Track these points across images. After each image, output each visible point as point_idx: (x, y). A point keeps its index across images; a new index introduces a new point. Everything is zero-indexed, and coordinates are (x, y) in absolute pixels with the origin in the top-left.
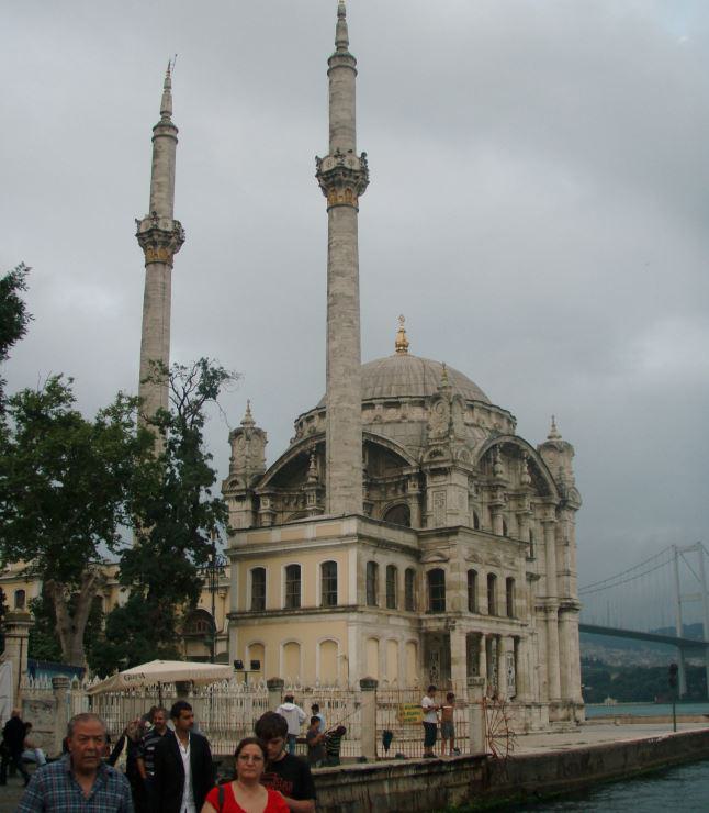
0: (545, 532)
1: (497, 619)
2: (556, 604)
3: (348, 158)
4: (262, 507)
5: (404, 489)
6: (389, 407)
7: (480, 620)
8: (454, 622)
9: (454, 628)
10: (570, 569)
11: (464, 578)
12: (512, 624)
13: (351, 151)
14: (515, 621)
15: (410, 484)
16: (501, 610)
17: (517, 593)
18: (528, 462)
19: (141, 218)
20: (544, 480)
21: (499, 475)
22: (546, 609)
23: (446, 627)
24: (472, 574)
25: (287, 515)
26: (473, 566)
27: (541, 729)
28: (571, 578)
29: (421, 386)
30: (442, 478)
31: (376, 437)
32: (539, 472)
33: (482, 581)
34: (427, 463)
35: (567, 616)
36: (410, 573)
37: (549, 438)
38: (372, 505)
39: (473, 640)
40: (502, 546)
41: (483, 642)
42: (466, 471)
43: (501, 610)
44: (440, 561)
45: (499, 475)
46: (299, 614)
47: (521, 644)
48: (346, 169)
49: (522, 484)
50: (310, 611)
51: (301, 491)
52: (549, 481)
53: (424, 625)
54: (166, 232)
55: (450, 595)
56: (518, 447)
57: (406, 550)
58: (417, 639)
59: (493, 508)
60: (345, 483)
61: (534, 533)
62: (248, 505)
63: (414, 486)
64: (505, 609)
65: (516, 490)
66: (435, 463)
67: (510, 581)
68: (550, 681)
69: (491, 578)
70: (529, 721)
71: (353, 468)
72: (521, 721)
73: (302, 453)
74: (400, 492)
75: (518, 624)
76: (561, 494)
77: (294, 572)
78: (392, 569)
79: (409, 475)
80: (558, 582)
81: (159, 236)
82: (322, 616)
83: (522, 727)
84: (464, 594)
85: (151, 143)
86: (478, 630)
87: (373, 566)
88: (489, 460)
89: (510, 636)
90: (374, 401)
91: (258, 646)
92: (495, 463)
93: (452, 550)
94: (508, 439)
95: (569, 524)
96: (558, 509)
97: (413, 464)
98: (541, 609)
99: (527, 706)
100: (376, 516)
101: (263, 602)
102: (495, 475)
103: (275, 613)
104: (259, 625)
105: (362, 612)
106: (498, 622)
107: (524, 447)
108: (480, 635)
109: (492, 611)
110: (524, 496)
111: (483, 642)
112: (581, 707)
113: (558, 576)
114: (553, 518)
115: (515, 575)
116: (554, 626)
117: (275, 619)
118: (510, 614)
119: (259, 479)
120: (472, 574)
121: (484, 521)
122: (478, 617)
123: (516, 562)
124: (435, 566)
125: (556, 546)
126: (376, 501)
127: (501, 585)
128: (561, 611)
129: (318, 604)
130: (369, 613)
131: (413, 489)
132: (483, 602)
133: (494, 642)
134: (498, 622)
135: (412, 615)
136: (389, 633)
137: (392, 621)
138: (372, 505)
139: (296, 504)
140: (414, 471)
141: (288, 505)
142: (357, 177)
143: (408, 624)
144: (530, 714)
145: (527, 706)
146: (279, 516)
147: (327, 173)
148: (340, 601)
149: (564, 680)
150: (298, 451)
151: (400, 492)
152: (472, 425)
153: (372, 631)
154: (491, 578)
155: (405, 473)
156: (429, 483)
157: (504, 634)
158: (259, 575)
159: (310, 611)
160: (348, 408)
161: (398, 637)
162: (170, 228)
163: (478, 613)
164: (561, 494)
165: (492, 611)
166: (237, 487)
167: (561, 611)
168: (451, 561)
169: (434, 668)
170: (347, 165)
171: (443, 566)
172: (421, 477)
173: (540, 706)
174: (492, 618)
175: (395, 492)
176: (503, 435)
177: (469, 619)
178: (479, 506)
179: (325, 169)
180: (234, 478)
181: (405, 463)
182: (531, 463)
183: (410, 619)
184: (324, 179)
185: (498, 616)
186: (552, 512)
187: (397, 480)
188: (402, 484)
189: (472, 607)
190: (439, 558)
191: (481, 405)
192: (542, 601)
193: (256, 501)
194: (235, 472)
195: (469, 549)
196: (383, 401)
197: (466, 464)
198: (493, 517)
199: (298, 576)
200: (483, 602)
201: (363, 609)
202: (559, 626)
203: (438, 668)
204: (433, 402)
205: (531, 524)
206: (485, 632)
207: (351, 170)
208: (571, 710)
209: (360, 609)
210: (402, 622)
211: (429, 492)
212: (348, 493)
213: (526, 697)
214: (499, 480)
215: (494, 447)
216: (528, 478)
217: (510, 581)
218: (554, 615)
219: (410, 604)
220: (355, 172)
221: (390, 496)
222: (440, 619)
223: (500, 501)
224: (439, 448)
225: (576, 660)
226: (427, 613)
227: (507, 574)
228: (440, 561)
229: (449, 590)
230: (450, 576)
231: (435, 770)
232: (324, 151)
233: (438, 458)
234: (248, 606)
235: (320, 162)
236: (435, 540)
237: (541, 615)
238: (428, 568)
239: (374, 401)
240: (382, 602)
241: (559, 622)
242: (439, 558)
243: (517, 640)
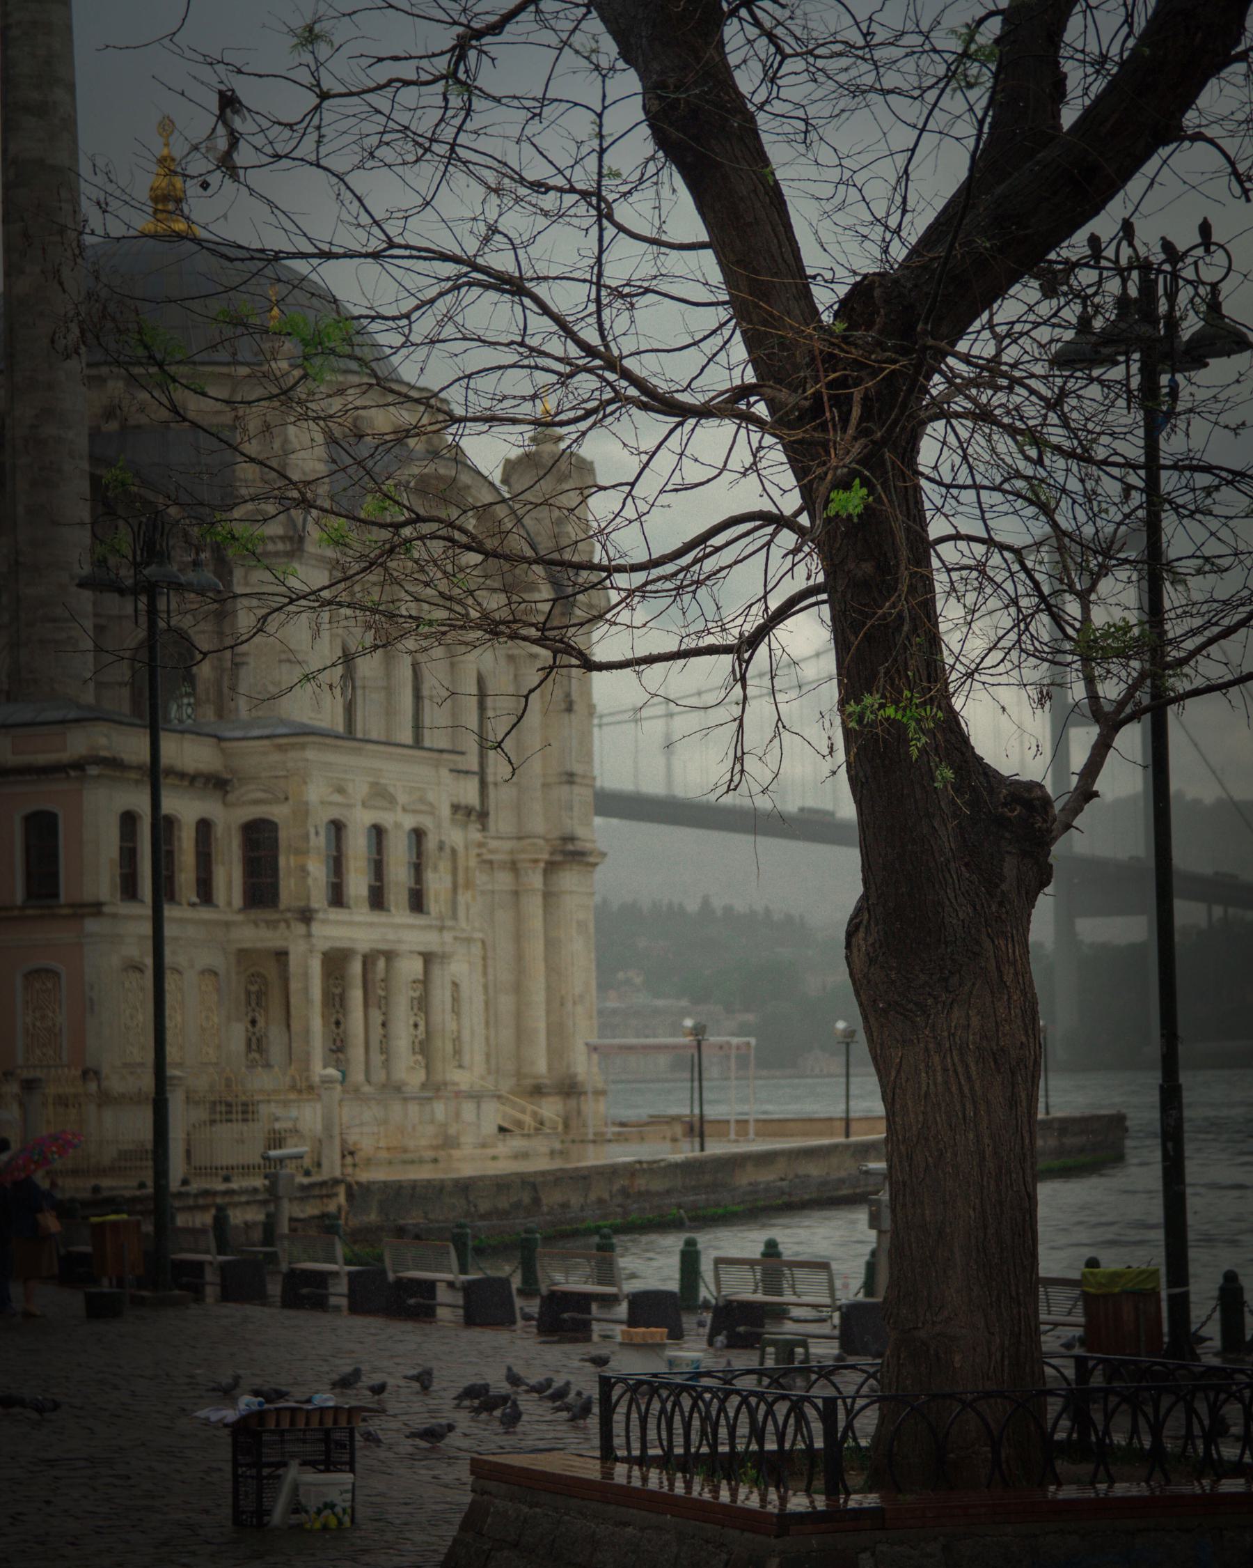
28: (577, 789)
33: (358, 846)
35: (569, 879)
36: (204, 826)
39: (335, 962)
41: (356, 967)
47: (436, 971)
64: (404, 897)
67: (418, 835)
68: (521, 1034)
70: (452, 1131)
75: (430, 927)
84: (318, 870)
109: (377, 900)
111: (356, 967)
115: (427, 822)
116: (534, 906)
118: (417, 902)
125: (545, 713)
128: (551, 868)
132: (358, 884)
133: (381, 963)
149: (558, 1033)
157: (404, 947)
165: (377, 900)
171: (278, 812)
189: (337, 897)
192: (508, 845)
200: (358, 884)
209: (106, 909)
218: (536, 880)
227: (409, 822)
237: (504, 880)
243: (428, 958)
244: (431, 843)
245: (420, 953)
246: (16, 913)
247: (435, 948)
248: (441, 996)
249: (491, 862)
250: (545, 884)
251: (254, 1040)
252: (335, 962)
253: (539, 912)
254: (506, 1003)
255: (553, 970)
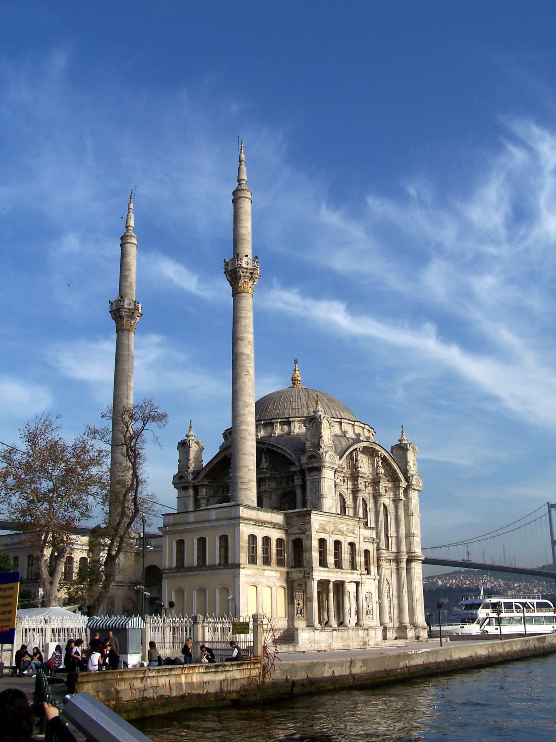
0: (396, 508)
1: (342, 570)
2: (405, 557)
3: (245, 259)
4: (199, 494)
5: (293, 481)
6: (284, 425)
7: (328, 571)
8: (309, 574)
9: (308, 578)
10: (415, 532)
11: (315, 544)
12: (353, 573)
13: (247, 256)
14: (355, 571)
15: (295, 477)
16: (346, 564)
17: (357, 552)
18: (382, 459)
19: (113, 300)
20: (395, 471)
21: (359, 469)
22: (397, 561)
23: (304, 577)
24: (322, 542)
25: (216, 499)
26: (323, 536)
27: (376, 644)
29: (305, 409)
30: (316, 473)
31: (273, 446)
32: (390, 465)
33: (330, 547)
34: (305, 464)
37: (399, 441)
38: (272, 492)
40: (344, 521)
42: (332, 468)
43: (346, 564)
44: (300, 533)
45: (359, 469)
46: (205, 570)
47: (360, 587)
48: (242, 268)
49: (377, 474)
50: (213, 567)
51: (224, 482)
52: (398, 471)
53: (290, 576)
54: (129, 309)
55: (306, 555)
56: (374, 450)
57: (275, 526)
58: (285, 585)
59: (355, 492)
60: (244, 480)
61: (388, 508)
62: (191, 492)
63: (298, 479)
65: (373, 479)
66: (313, 462)
67: (352, 545)
69: (337, 544)
70: (366, 640)
71: (249, 470)
72: (360, 639)
73: (226, 457)
74: (290, 483)
76: (407, 479)
77: (202, 542)
78: (266, 540)
79: (294, 472)
80: (406, 541)
81: (125, 312)
82: (219, 571)
83: (362, 643)
84: (315, 555)
85: (120, 248)
86: (327, 578)
87: (253, 538)
88: (352, 459)
89: (351, 582)
90: (273, 421)
91: (180, 592)
92: (356, 461)
93: (307, 526)
94: (365, 445)
95: (413, 500)
96: (406, 491)
97: (297, 463)
98: (394, 560)
99: (365, 629)
100: (275, 498)
101: (183, 561)
102: (356, 469)
103: (191, 569)
104: (181, 576)
105: (244, 568)
106: (342, 572)
107: (377, 448)
108: (329, 581)
110: (379, 482)
112: (424, 629)
113: (406, 537)
114: (402, 496)
115: (355, 541)
117: (190, 573)
118: (353, 566)
119: (197, 473)
120: (322, 542)
121: (349, 501)
122: (327, 569)
123: (356, 532)
124: (297, 536)
126: (274, 489)
127: (345, 549)
128: (409, 561)
129: (217, 562)
130: (250, 568)
131: (297, 482)
132: (331, 559)
134: (342, 572)
135: (284, 569)
136: (264, 581)
137: (267, 573)
138: (272, 492)
139: (223, 491)
140: (298, 469)
141: (217, 491)
142: (251, 273)
143: (278, 575)
144: (368, 635)
145: (365, 629)
146: (211, 499)
147: (231, 271)
148: (230, 562)
150: (223, 455)
151: (290, 483)
152: (341, 436)
153: (253, 580)
154: (337, 544)
155: (293, 469)
156: (308, 477)
158: (181, 543)
159: (213, 567)
160: (245, 430)
161: (271, 584)
162: (132, 307)
163: (328, 567)
164: (407, 479)
165: (338, 565)
166: (183, 480)
167: (409, 561)
168: (307, 533)
169: (299, 604)
170: (244, 265)
171: (302, 536)
172: (302, 473)
173: (376, 629)
174: (338, 570)
175: (287, 482)
176: (363, 441)
177: (320, 571)
178: (346, 491)
179: (230, 268)
180: (181, 474)
181: (292, 463)
182: (384, 459)
183: (280, 572)
184: (230, 275)
185: (342, 568)
186: (401, 491)
187: (287, 475)
188: (290, 478)
189: (323, 563)
190: (300, 531)
191: (347, 421)
193: (196, 488)
194: (181, 470)
195: (320, 524)
196: (279, 420)
197: (333, 463)
198: (355, 499)
199: (204, 545)
200: (331, 559)
201: (245, 566)
202: (407, 573)
203: (301, 604)
204: (310, 422)
205: (386, 500)
206: (333, 580)
207: (247, 269)
208: (417, 630)
209: (242, 566)
210: (273, 574)
211: (308, 483)
212: (246, 487)
213: (366, 621)
214: (358, 472)
215: (355, 450)
216: (382, 471)
217: (352, 545)
218: (404, 565)
219: (280, 563)
220: (250, 269)
221: (284, 485)
222: (300, 572)
223: (361, 486)
224: (314, 453)
225: (421, 595)
226: (292, 567)
227: (350, 540)
228: (300, 533)
229: (306, 552)
230: (305, 543)
231: (220, 669)
232: (229, 257)
233: (313, 460)
234: (174, 565)
235: (227, 264)
236: (296, 519)
237: (394, 565)
238: (293, 538)
239: (273, 421)
240: (260, 561)
241: (406, 569)
242: (300, 531)
243: (357, 584)
244: (357, 547)
245: (354, 582)
246: (217, 567)
247: (360, 580)
248: (362, 596)
249: (390, 560)
250: (406, 566)
251: (299, 610)
252: (324, 584)
253: (405, 574)
254: (395, 601)
255: (410, 592)
